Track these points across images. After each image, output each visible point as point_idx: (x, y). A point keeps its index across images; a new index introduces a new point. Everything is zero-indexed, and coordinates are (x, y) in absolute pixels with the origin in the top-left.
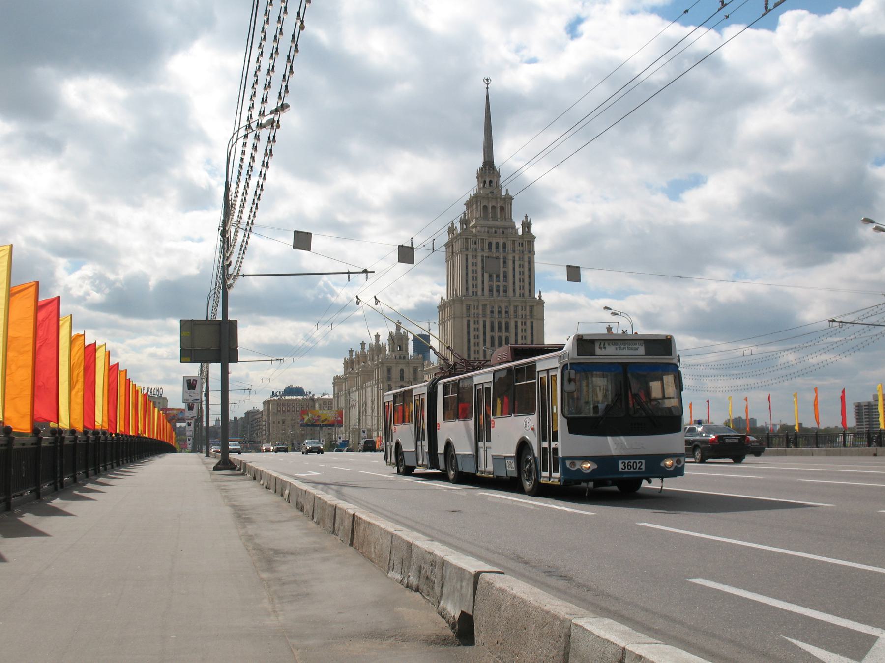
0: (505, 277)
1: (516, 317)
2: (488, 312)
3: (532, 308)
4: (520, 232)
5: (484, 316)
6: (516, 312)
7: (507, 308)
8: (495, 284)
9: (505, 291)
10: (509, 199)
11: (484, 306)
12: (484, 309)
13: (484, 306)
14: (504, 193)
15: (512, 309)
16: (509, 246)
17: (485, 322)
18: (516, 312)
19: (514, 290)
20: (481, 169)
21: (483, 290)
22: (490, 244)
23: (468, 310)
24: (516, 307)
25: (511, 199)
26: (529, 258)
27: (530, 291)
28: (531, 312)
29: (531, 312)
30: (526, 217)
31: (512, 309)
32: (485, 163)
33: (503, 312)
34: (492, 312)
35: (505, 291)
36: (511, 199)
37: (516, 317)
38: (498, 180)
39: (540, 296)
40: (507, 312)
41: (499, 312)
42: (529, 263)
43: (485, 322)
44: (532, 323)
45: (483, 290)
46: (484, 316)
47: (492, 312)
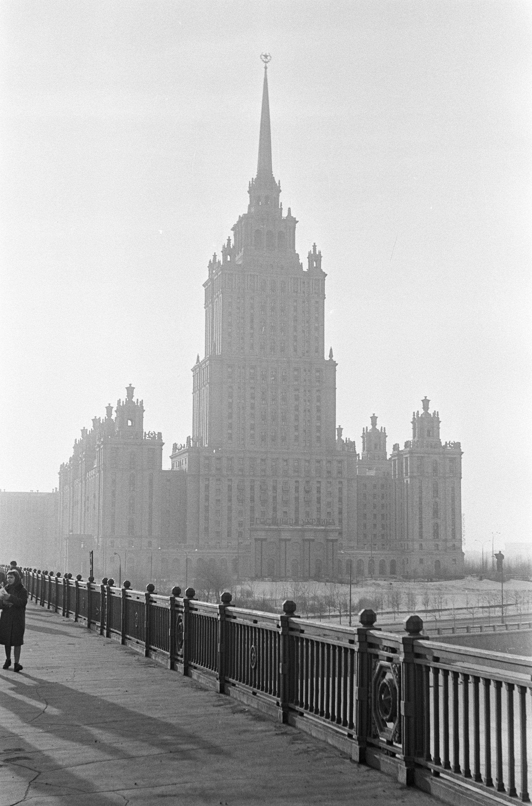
4: (305, 268)
14: (285, 214)
30: (315, 246)
36: (295, 222)
38: (278, 196)
39: (331, 355)
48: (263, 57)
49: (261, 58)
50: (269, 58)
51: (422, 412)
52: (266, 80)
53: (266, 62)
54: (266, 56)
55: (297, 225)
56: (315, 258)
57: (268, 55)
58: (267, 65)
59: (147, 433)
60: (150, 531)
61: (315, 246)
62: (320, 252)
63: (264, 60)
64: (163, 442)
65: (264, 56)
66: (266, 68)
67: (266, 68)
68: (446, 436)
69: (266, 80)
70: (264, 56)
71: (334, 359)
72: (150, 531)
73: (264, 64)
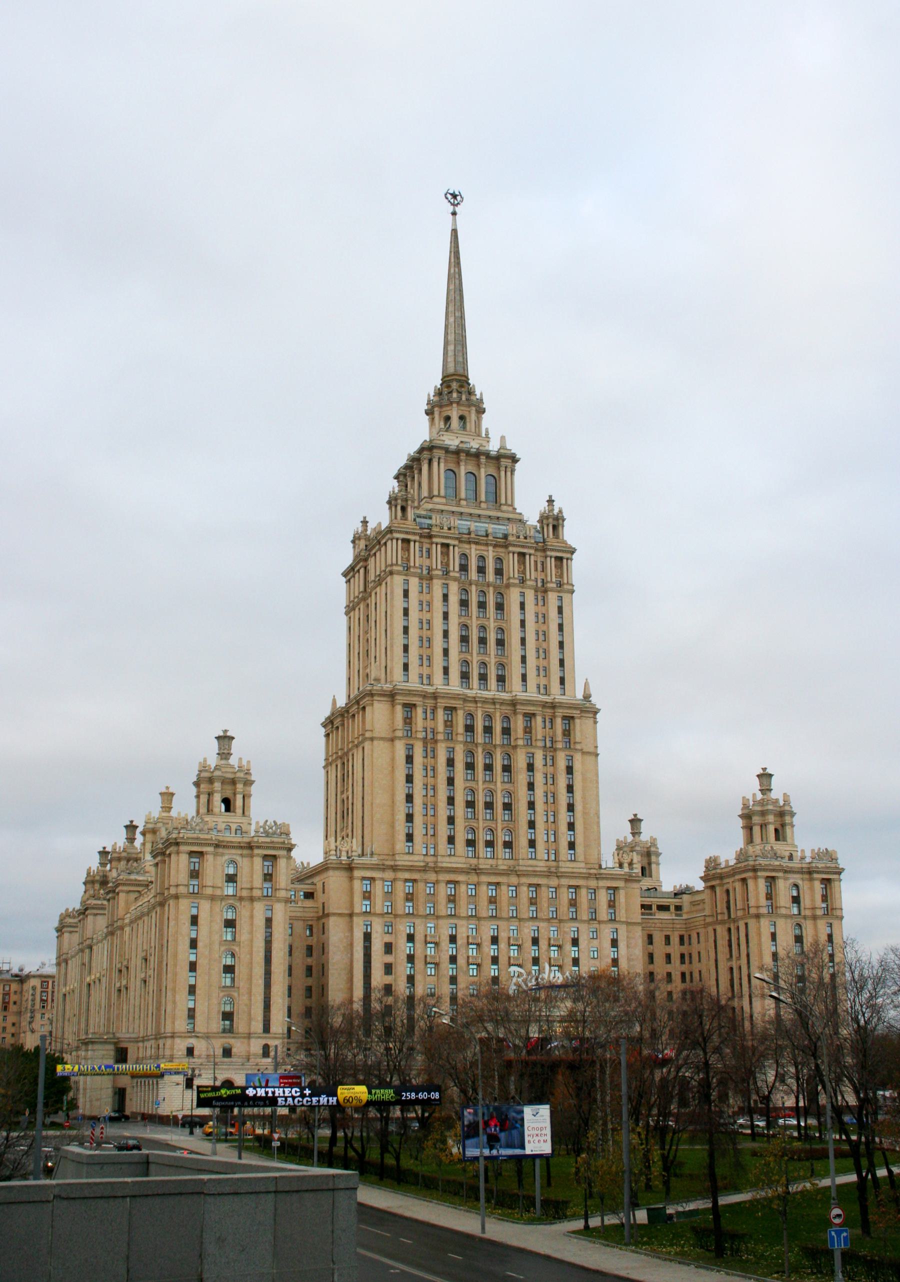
0: (500, 643)
1: (530, 743)
2: (461, 729)
3: (569, 719)
5: (450, 736)
6: (528, 730)
7: (507, 718)
8: (475, 660)
9: (501, 679)
10: (505, 461)
11: (451, 710)
12: (449, 724)
13: (451, 710)
15: (519, 724)
16: (511, 565)
17: (451, 750)
18: (528, 730)
19: (524, 678)
20: (439, 393)
21: (446, 671)
22: (464, 556)
23: (408, 721)
24: (530, 716)
25: (514, 459)
26: (560, 599)
27: (562, 681)
28: (567, 733)
29: (567, 733)
30: (551, 501)
31: (519, 724)
32: (447, 380)
33: (498, 728)
34: (470, 728)
35: (501, 679)
36: (514, 459)
37: (530, 743)
39: (587, 697)
40: (506, 731)
41: (488, 730)
42: (560, 610)
43: (451, 750)
44: (571, 759)
45: (446, 671)
46: (450, 736)
47: (470, 728)
48: (449, 197)
49: (447, 198)
50: (459, 198)
51: (630, 838)
52: (454, 232)
53: (453, 204)
54: (454, 196)
55: (517, 465)
56: (553, 521)
57: (457, 193)
58: (457, 209)
59: (261, 824)
60: (267, 1028)
61: (551, 501)
62: (560, 511)
63: (452, 201)
64: (293, 842)
65: (451, 194)
66: (454, 214)
67: (454, 214)
68: (805, 841)
69: (454, 232)
70: (451, 194)
71: (593, 699)
72: (267, 1028)
73: (451, 209)
